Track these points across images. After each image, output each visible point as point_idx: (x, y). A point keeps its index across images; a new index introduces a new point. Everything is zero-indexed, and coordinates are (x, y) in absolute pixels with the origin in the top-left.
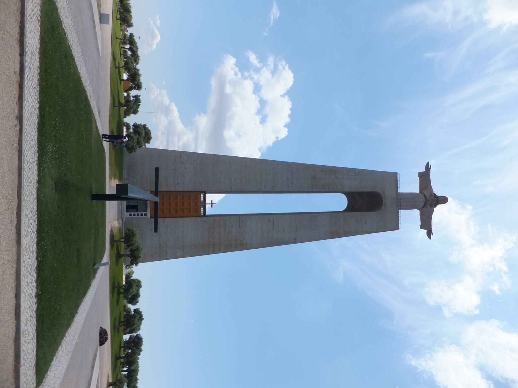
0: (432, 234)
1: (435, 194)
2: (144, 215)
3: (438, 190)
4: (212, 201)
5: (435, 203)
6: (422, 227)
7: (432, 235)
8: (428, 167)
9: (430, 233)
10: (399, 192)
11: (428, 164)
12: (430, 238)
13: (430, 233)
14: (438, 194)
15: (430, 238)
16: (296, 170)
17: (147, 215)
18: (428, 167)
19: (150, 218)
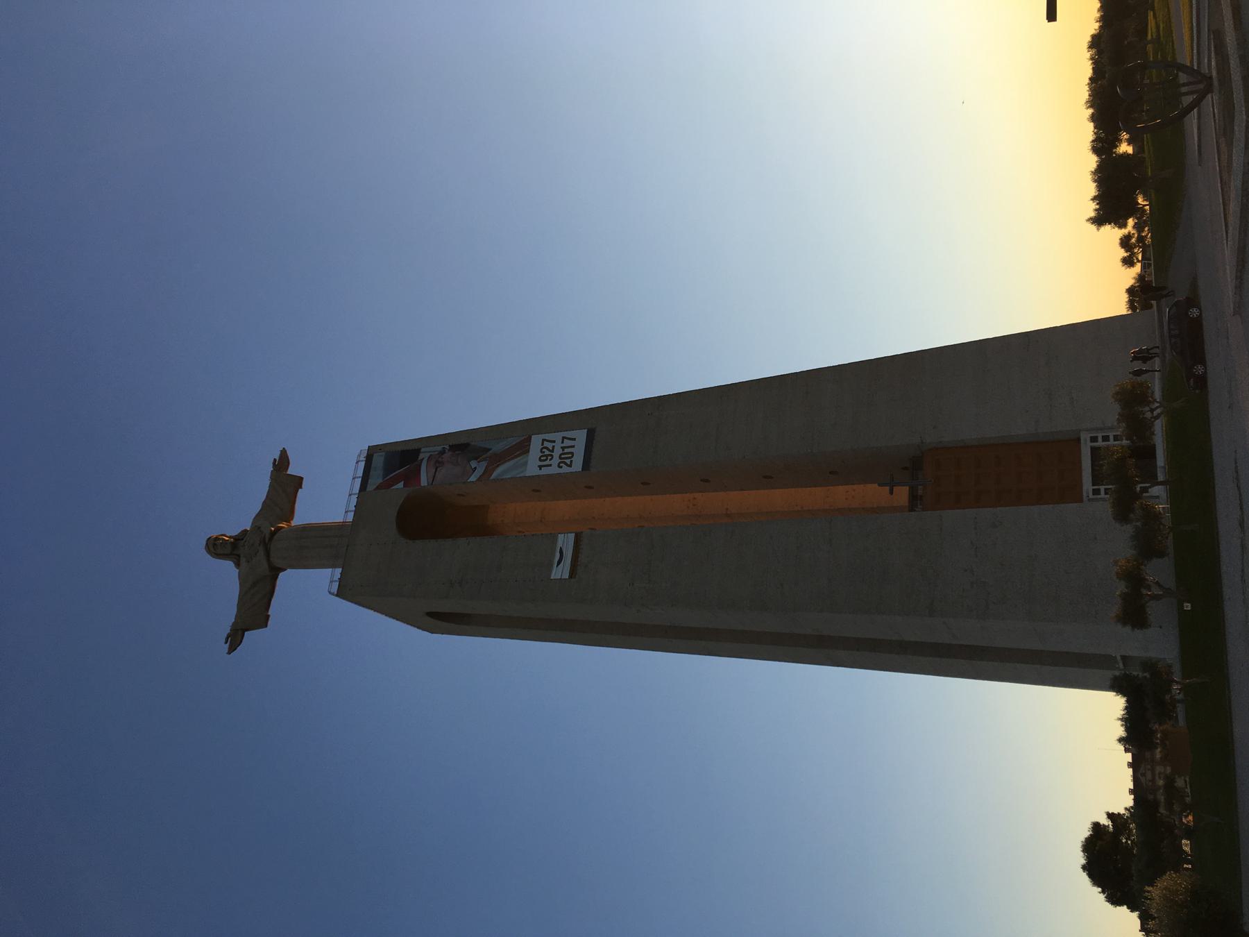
0: (274, 463)
1: (238, 565)
2: (1100, 439)
3: (227, 575)
4: (891, 492)
5: (242, 539)
6: (298, 482)
7: (275, 460)
8: (235, 639)
9: (282, 462)
10: (340, 570)
11: (232, 649)
12: (284, 454)
13: (282, 462)
14: (229, 565)
15: (284, 454)
16: (633, 584)
17: (1089, 439)
18: (235, 639)
19: (1079, 440)
